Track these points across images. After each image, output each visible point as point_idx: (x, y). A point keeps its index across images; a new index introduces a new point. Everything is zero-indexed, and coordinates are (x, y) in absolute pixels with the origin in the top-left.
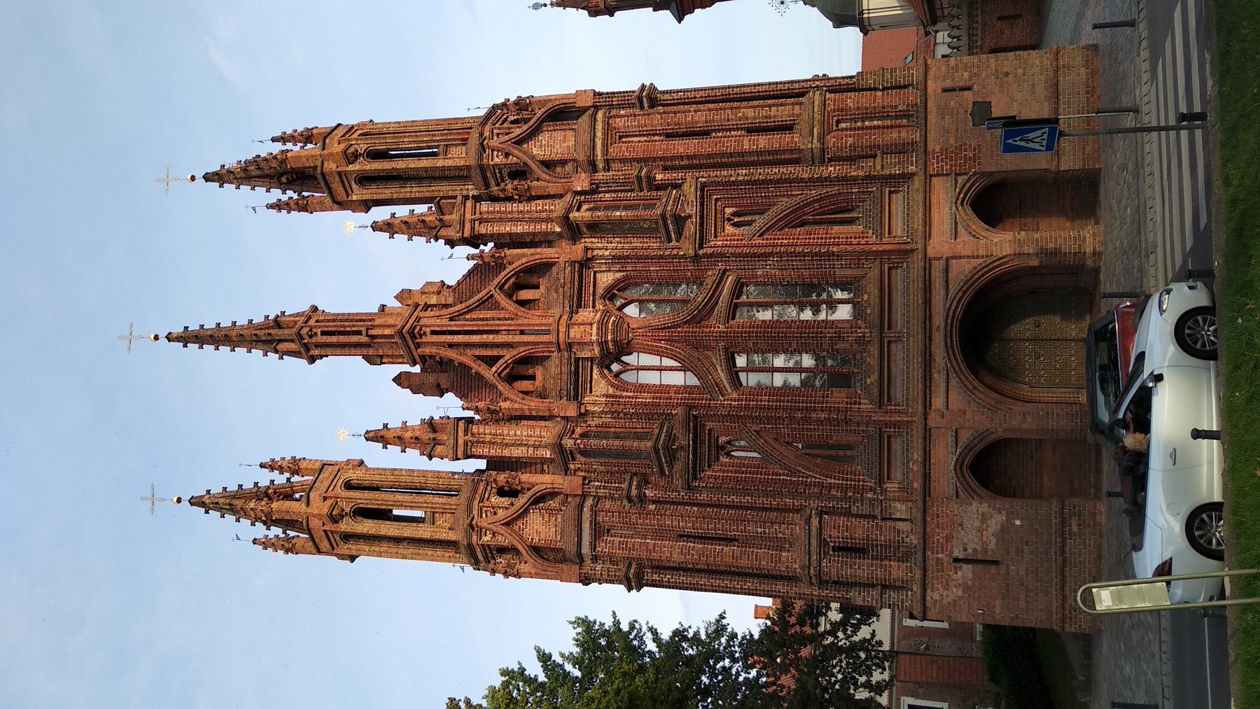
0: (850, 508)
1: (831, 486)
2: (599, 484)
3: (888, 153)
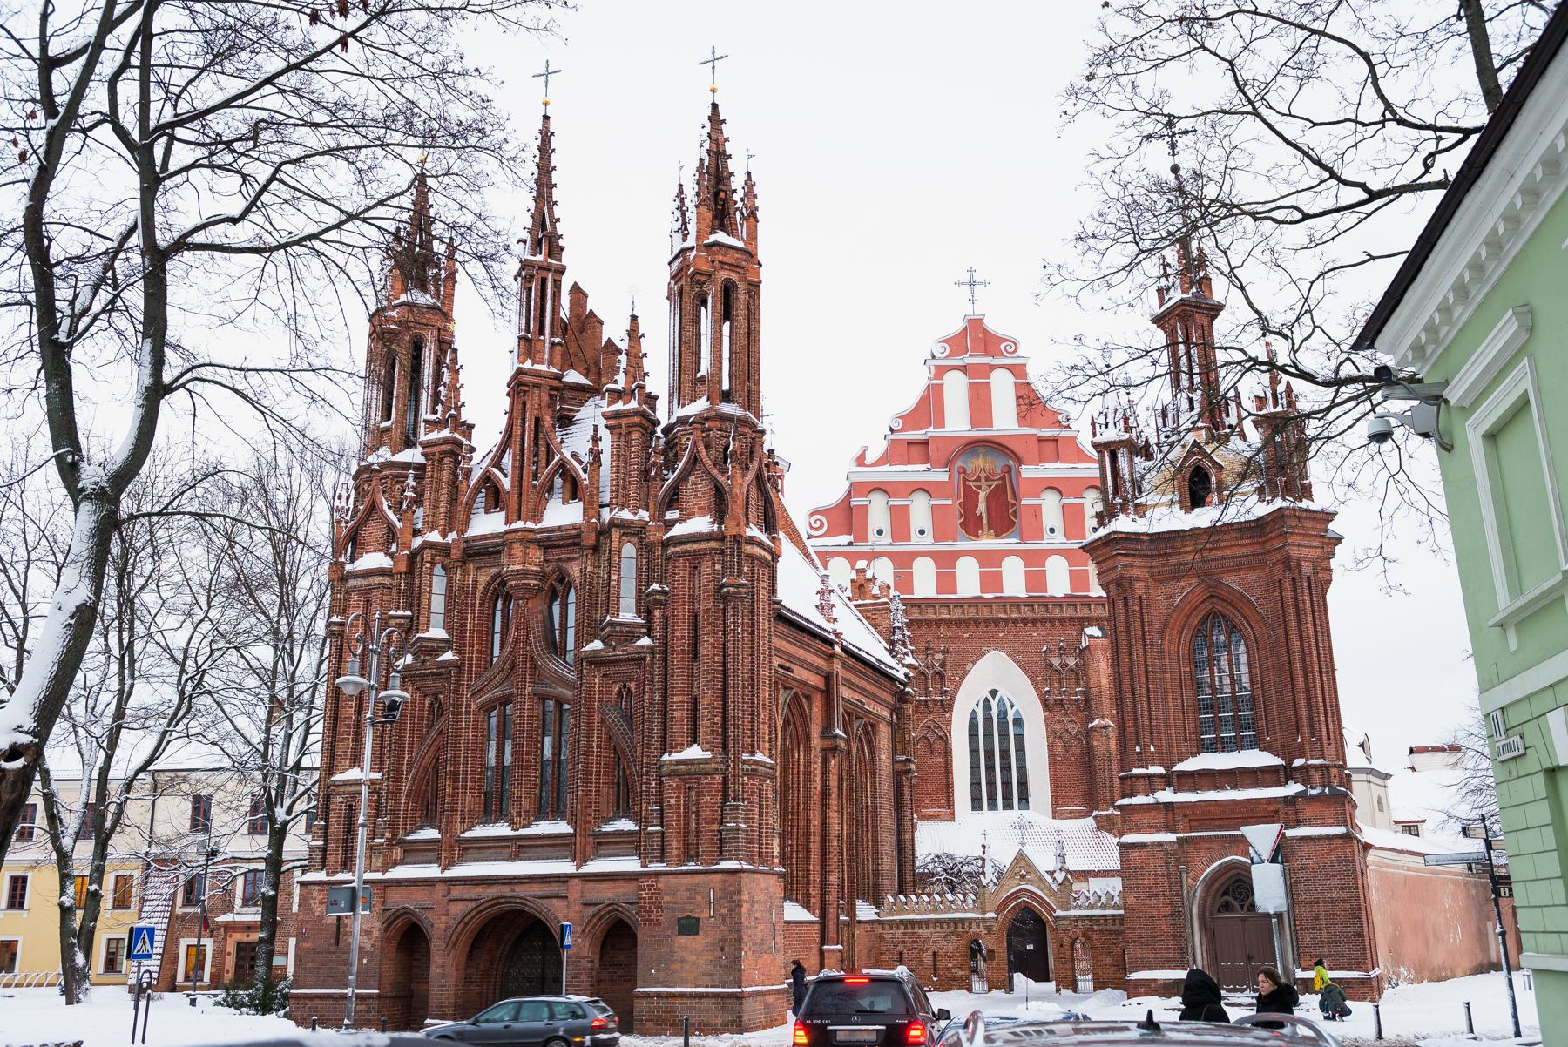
1: (397, 800)
3: (663, 837)
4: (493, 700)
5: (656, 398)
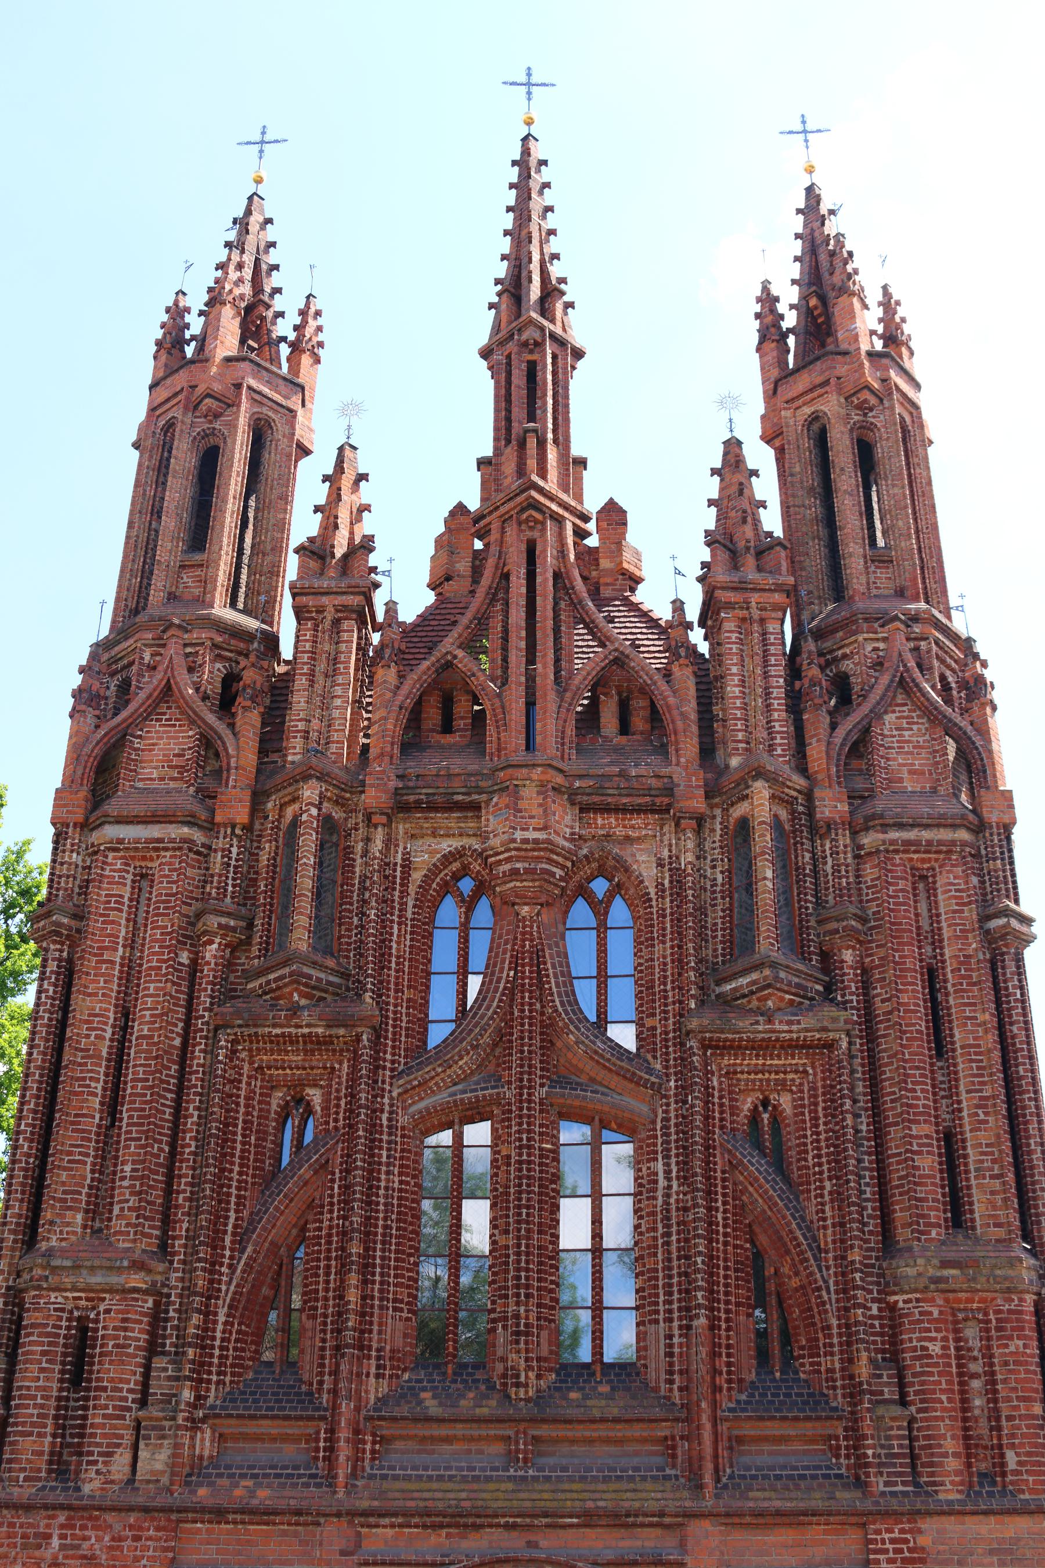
0: (164, 1353)
1: (208, 1313)
2: (234, 855)
3: (910, 1429)
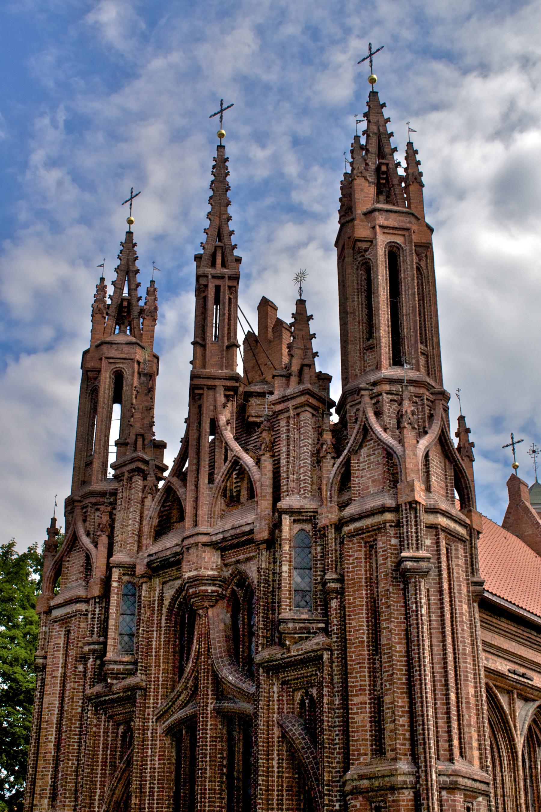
2: (97, 612)
4: (181, 722)
5: (328, 379)
